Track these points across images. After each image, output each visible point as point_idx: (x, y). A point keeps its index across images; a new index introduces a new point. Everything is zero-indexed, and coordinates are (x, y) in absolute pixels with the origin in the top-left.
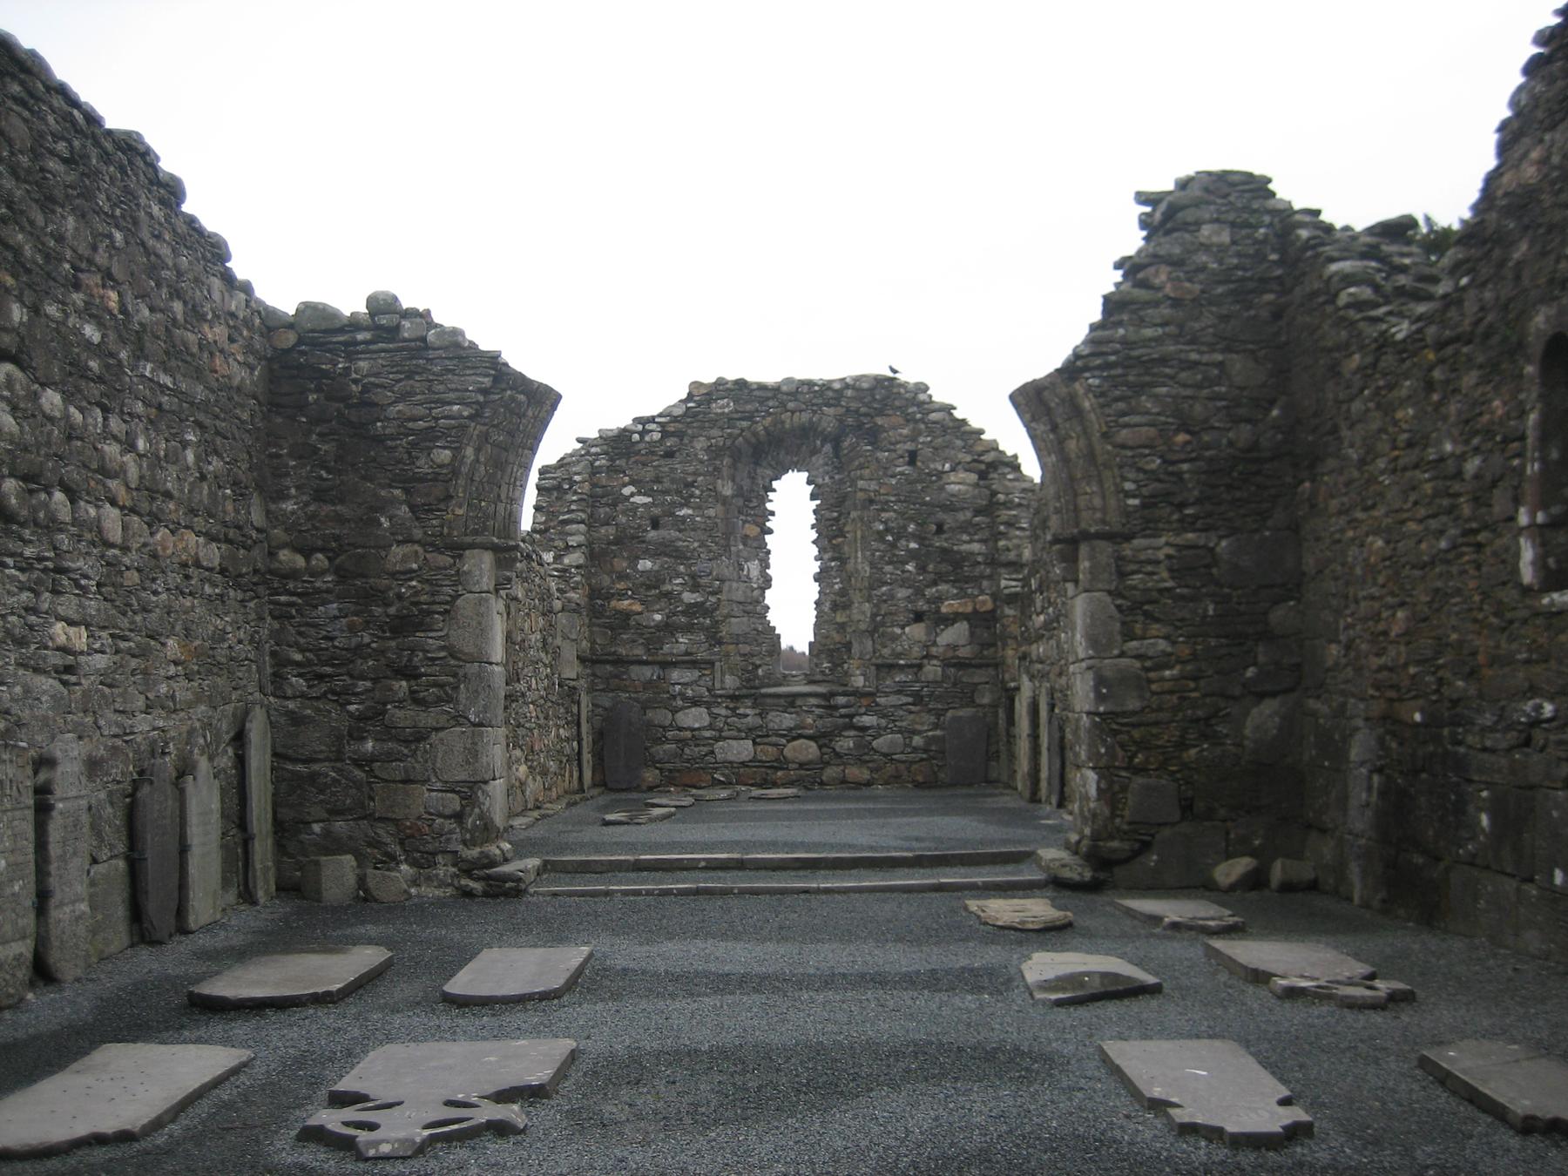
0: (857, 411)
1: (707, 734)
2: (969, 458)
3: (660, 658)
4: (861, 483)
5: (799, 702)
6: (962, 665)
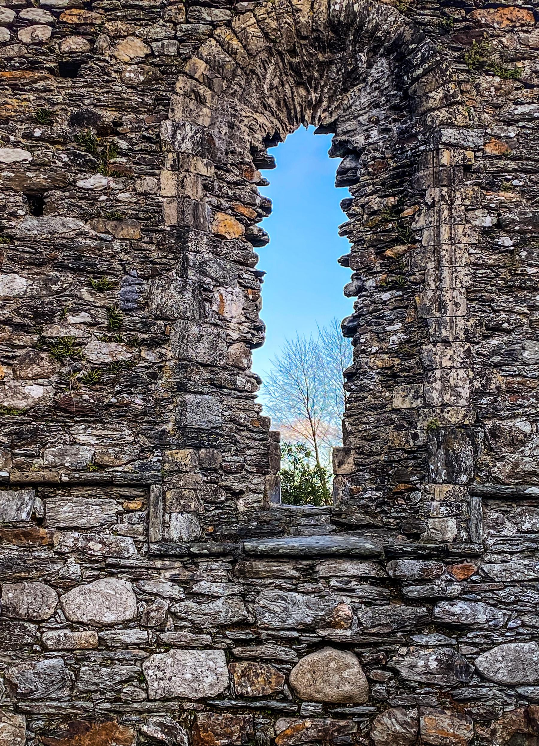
3: (32, 476)
4: (449, 134)
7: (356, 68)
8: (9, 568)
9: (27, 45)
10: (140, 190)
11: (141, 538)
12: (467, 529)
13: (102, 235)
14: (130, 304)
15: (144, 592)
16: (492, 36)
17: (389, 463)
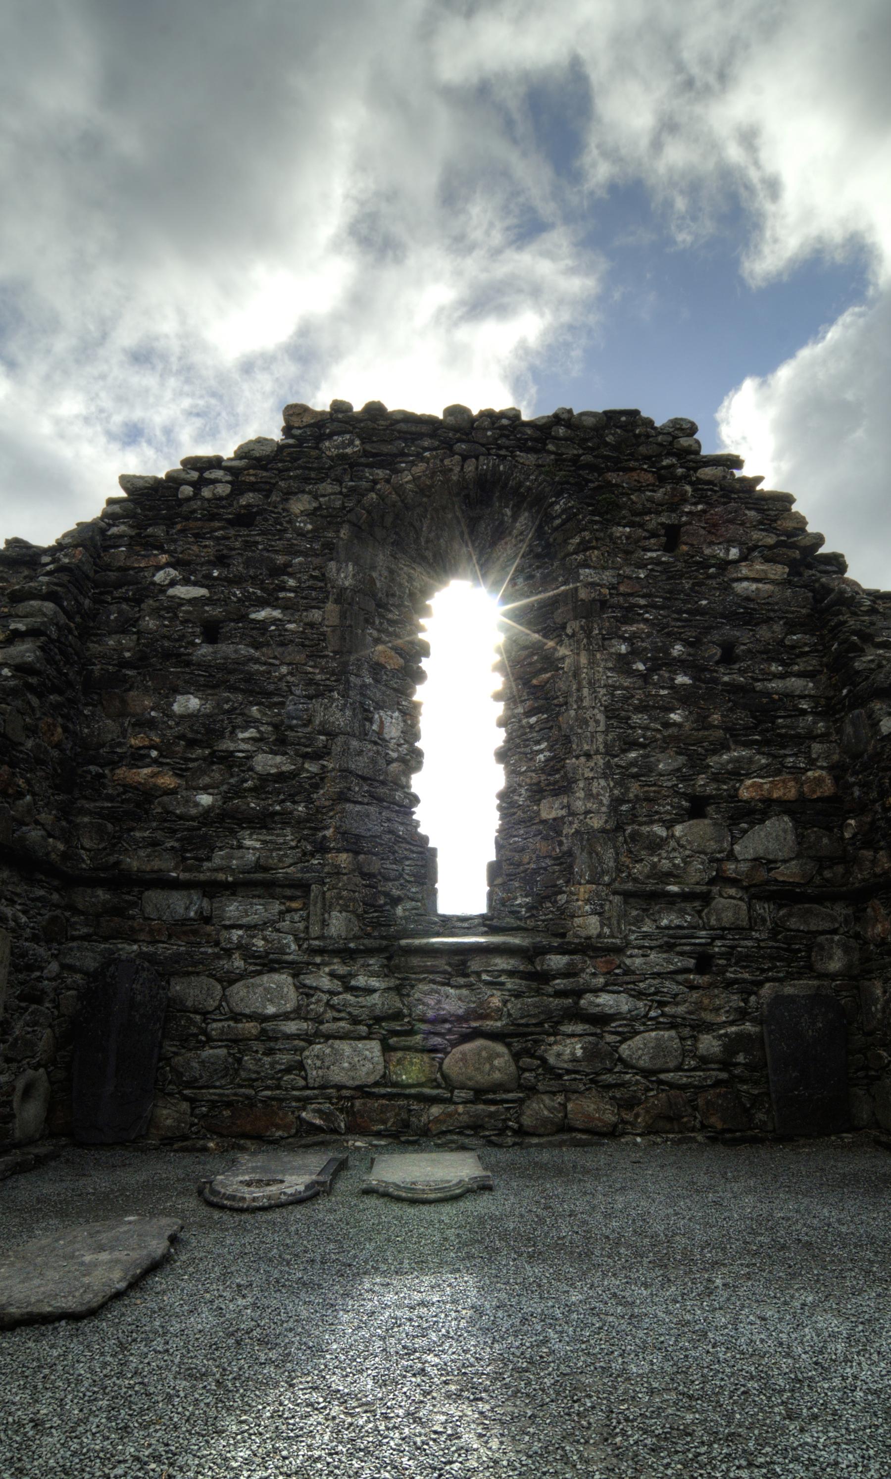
0: (575, 459)
1: (291, 1027)
2: (771, 540)
5: (475, 965)
6: (785, 896)
7: (502, 523)
8: (177, 962)
9: (208, 500)
10: (306, 620)
11: (302, 935)
12: (609, 926)
13: (271, 661)
14: (295, 722)
15: (305, 986)
16: (623, 494)
17: (536, 872)
